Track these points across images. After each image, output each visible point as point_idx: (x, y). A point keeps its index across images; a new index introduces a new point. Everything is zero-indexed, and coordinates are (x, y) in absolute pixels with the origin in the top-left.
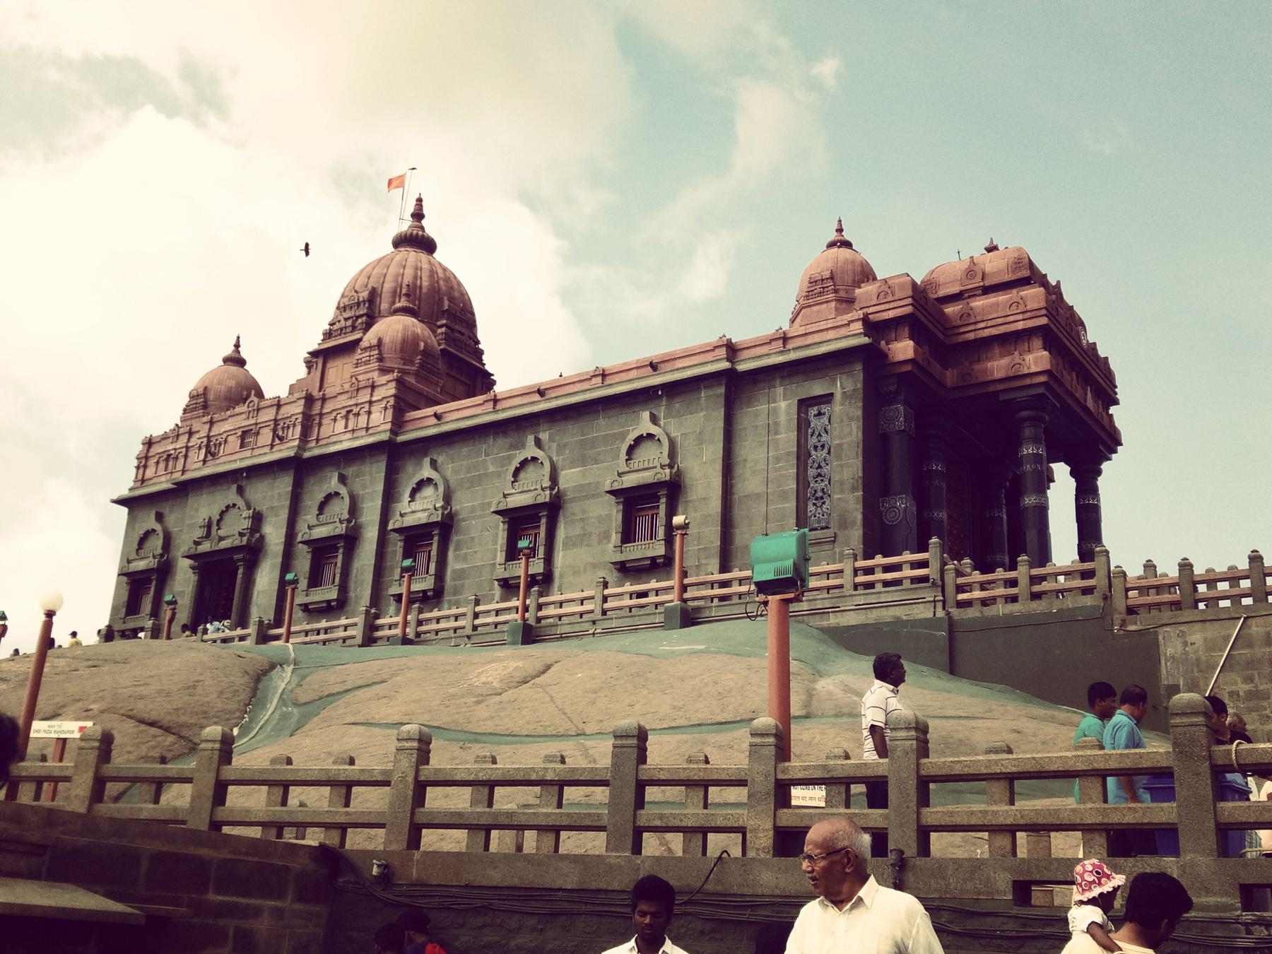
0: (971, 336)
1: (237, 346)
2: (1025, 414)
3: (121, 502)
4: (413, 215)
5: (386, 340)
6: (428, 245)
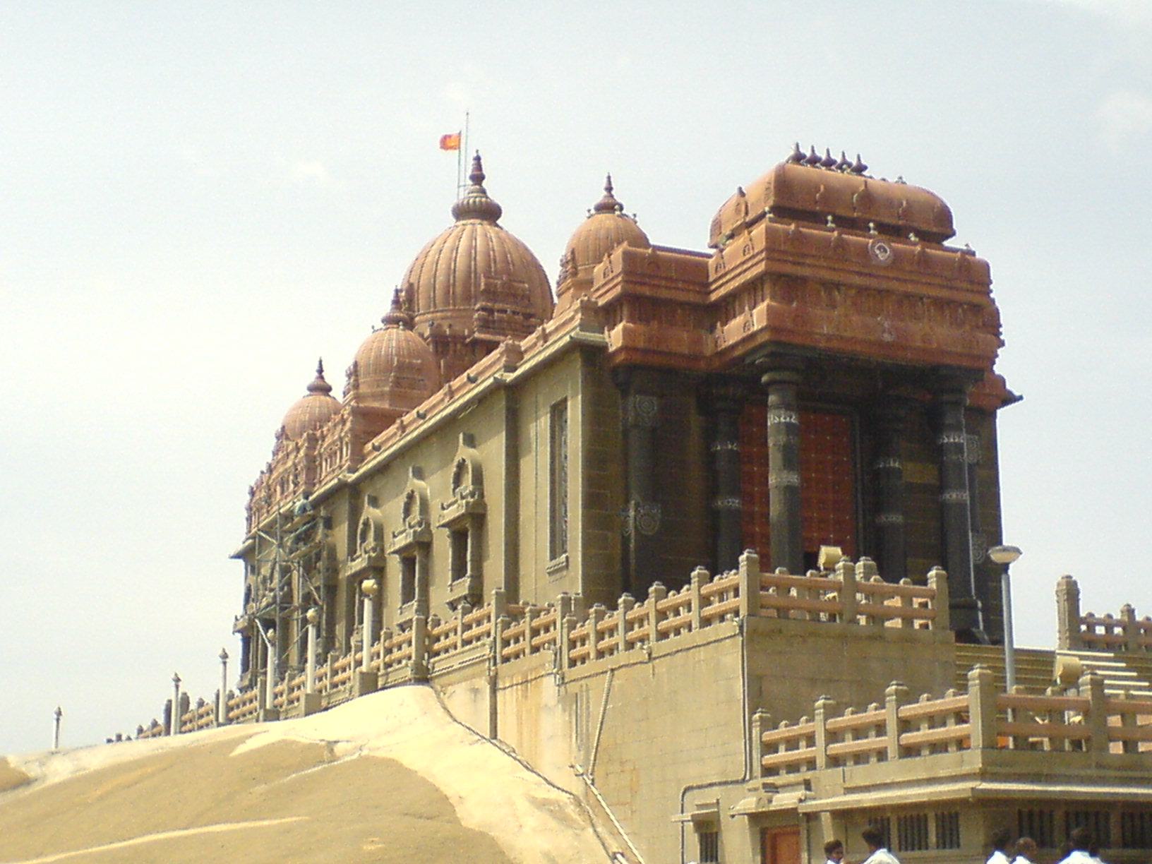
0: (722, 291)
1: (321, 371)
2: (765, 379)
3: (237, 556)
4: (473, 178)
5: (361, 363)
6: (490, 213)
